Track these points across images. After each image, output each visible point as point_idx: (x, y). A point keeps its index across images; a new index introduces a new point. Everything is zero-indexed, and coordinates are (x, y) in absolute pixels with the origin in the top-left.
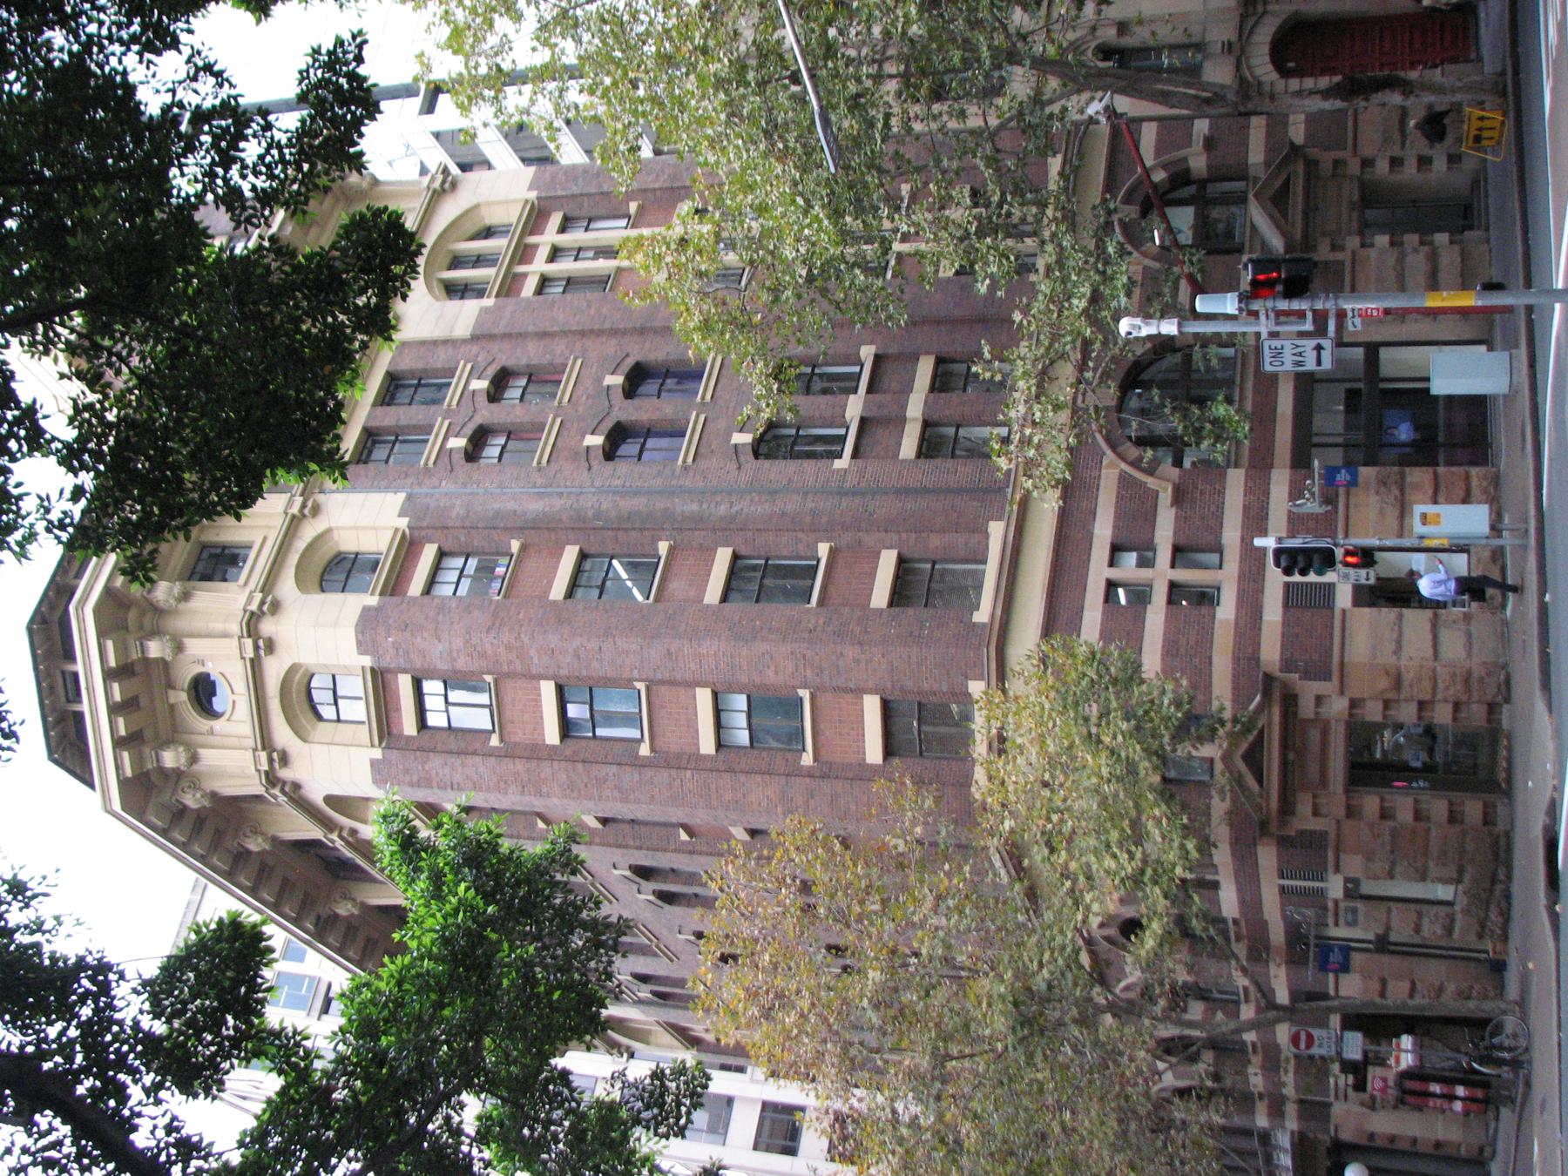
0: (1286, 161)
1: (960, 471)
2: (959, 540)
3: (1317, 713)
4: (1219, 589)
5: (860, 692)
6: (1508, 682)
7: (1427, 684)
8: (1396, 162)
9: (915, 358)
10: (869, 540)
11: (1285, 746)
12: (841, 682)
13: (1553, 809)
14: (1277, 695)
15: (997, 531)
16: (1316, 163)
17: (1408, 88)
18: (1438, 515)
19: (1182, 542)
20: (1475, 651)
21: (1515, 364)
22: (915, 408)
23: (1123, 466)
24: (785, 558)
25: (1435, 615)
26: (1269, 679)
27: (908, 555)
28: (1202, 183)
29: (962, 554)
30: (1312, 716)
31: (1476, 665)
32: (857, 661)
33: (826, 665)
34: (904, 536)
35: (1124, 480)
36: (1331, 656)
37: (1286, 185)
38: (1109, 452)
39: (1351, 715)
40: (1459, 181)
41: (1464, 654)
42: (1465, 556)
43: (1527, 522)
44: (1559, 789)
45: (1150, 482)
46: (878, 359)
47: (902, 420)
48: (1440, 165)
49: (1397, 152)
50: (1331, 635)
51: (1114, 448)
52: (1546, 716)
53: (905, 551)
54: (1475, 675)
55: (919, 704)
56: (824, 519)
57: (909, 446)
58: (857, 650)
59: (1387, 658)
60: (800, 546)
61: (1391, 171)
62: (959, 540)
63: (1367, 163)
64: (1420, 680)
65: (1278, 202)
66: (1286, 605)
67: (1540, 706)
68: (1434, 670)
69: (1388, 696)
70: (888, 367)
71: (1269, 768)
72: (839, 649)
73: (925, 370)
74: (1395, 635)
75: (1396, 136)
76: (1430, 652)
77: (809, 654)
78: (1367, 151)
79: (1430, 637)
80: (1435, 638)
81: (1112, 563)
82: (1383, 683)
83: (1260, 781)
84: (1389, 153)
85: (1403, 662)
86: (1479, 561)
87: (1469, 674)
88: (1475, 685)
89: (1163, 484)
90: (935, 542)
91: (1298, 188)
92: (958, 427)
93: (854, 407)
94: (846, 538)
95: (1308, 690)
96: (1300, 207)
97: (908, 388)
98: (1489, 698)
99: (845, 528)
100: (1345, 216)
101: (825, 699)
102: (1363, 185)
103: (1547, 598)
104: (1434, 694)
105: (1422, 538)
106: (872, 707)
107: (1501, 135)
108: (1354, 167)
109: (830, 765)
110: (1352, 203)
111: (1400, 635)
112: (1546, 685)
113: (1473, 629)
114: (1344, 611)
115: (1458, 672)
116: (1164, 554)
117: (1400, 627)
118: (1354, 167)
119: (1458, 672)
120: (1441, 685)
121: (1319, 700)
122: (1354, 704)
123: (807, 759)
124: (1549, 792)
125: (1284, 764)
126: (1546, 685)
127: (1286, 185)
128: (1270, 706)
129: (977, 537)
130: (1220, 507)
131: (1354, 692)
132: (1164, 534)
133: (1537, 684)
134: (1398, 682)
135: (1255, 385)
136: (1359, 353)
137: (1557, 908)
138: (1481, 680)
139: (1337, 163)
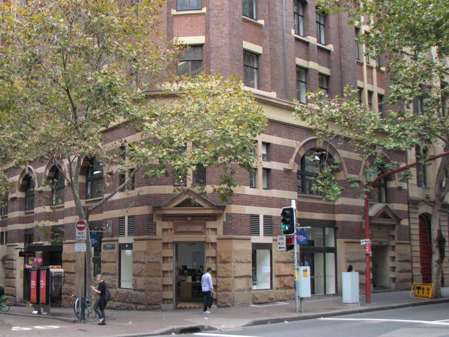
0: (396, 217)
1: (292, 83)
2: (267, 80)
3: (208, 229)
4: (254, 188)
5: (207, 34)
6: (227, 306)
7: (224, 274)
8: (393, 258)
9: (329, 67)
10: (266, 41)
11: (193, 216)
12: (212, 26)
13: (210, 329)
14: (217, 212)
15: (273, 95)
16: (394, 229)
17: (440, 262)
18: (306, 276)
19: (272, 173)
20: (238, 293)
21: (355, 305)
22: (312, 65)
23: (297, 149)
24: (256, 6)
25: (250, 277)
26: (223, 208)
27: (260, 58)
28: (385, 186)
29: (262, 81)
30: (207, 227)
31: (234, 294)
32: (222, 32)
33: (219, 18)
34: (269, 56)
35: (293, 149)
36: (234, 234)
37: (388, 217)
38: (301, 144)
39: (208, 243)
40: (387, 282)
41: (237, 289)
42: (269, 287)
43: (305, 312)
44: (221, 332)
45: (292, 160)
46: (329, 52)
47: (308, 59)
48: (392, 275)
49: (397, 259)
50: (241, 234)
51: (303, 145)
52: (243, 324)
53: (262, 56)
54: (229, 293)
55: (202, 60)
56: (274, 23)
57: (300, 62)
58: (227, 33)
59: (235, 257)
60: (262, 12)
61: (391, 257)
62: (267, 80)
63: (393, 247)
64: (226, 271)
65: (384, 215)
66: (252, 216)
67: (247, 321)
68: (230, 277)
69: (218, 258)
70: (325, 55)
71: (182, 209)
72: (227, 25)
73: (325, 71)
74: (243, 260)
75: (402, 259)
76: (237, 275)
77: (224, 12)
78: (398, 248)
79: (243, 275)
80: (242, 277)
81: (264, 143)
82: (224, 257)
83: (177, 206)
84: (397, 256)
85: (233, 264)
86: (269, 293)
87: (230, 291)
88: (224, 293)
89: (292, 165)
90: (266, 70)
91: (387, 222)
92: (305, 83)
93: (312, 40)
94: (267, 32)
95: (219, 225)
96: (381, 222)
97: (320, 64)
98: (219, 299)
99: (271, 32)
100: (377, 239)
101: (202, 18)
102: (387, 246)
103: (286, 322)
104: (219, 277)
105: (298, 270)
106: (200, 40)
107: (420, 296)
108: (392, 243)
109: (172, 22)
110: (381, 242)
111: (243, 263)
112: (256, 323)
113: (246, 292)
114: (249, 239)
115: (230, 287)
116: (267, 165)
117: (246, 263)
118: (392, 243)
119: (230, 287)
120: (224, 280)
121: (215, 230)
122: (214, 244)
123: (174, 12)
124: (218, 328)
125: (185, 216)
126: (256, 323)
127: (388, 217)
128: (212, 209)
129: (269, 87)
130: (284, 189)
131: (219, 243)
132: (274, 165)
133: (255, 320)
134: (224, 262)
135: (322, 204)
136: (333, 245)
137: (173, 333)
138: (227, 296)
139: (393, 236)
